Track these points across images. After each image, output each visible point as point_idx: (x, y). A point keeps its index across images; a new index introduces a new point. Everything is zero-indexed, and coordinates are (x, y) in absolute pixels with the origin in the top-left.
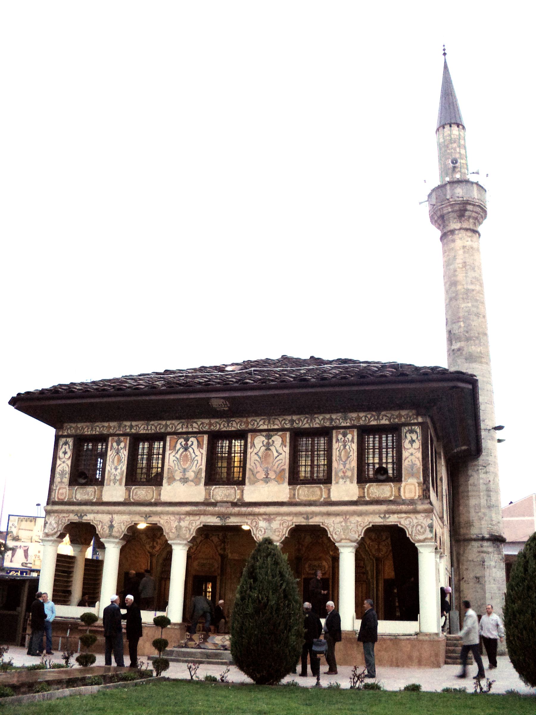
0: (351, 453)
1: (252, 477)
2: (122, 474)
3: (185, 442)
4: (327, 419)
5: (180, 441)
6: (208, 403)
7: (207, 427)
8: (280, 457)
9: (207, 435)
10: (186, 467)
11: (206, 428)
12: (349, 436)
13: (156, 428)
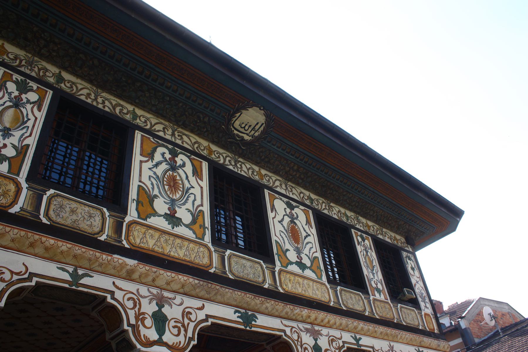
0: (374, 264)
1: (281, 253)
2: (22, 151)
3: (170, 156)
4: (343, 214)
5: (160, 150)
6: (238, 110)
7: (205, 152)
8: (308, 239)
9: (207, 163)
10: (174, 197)
11: (205, 153)
12: (366, 241)
13: (114, 109)
